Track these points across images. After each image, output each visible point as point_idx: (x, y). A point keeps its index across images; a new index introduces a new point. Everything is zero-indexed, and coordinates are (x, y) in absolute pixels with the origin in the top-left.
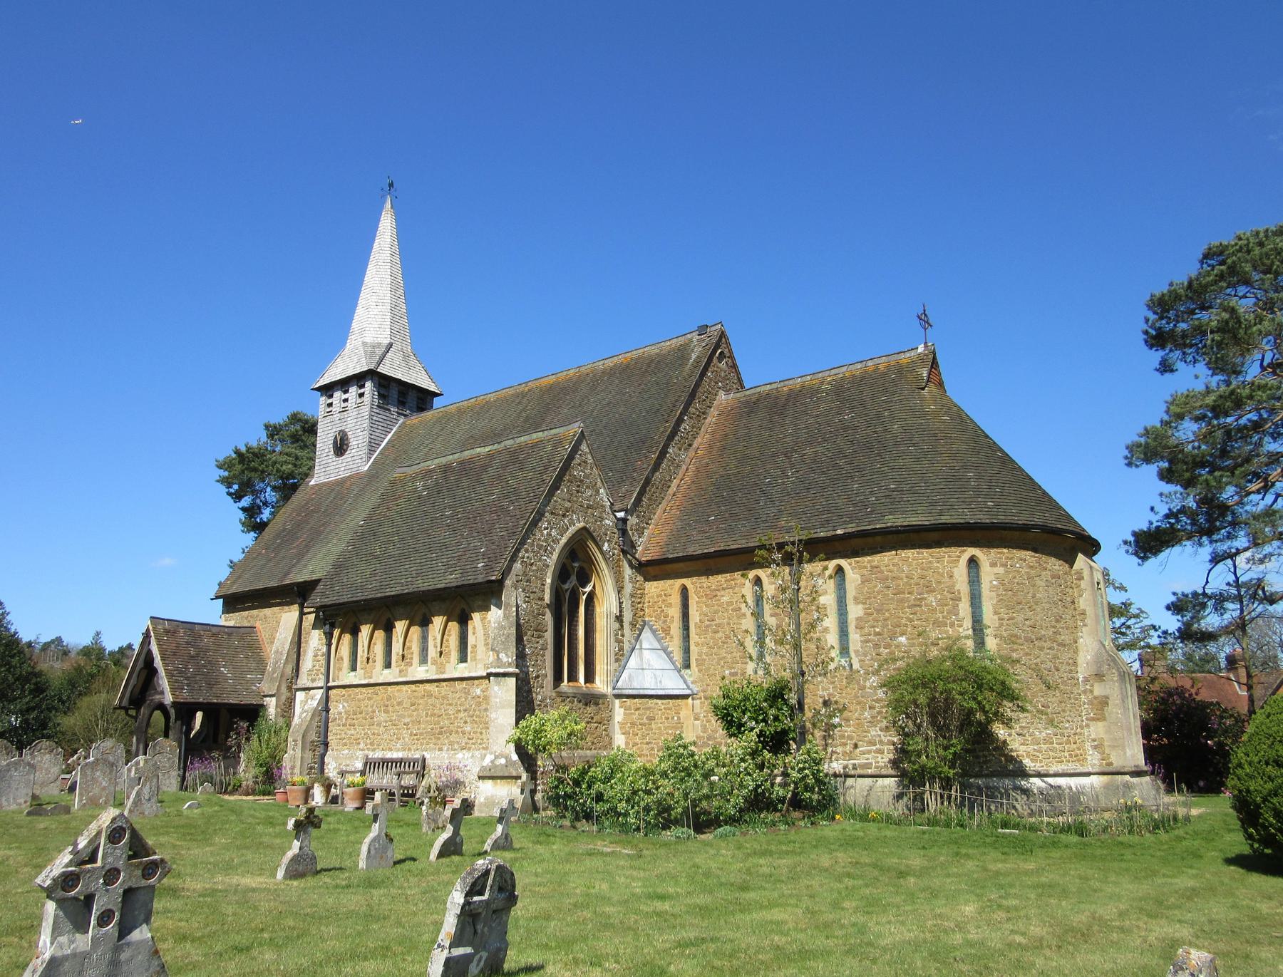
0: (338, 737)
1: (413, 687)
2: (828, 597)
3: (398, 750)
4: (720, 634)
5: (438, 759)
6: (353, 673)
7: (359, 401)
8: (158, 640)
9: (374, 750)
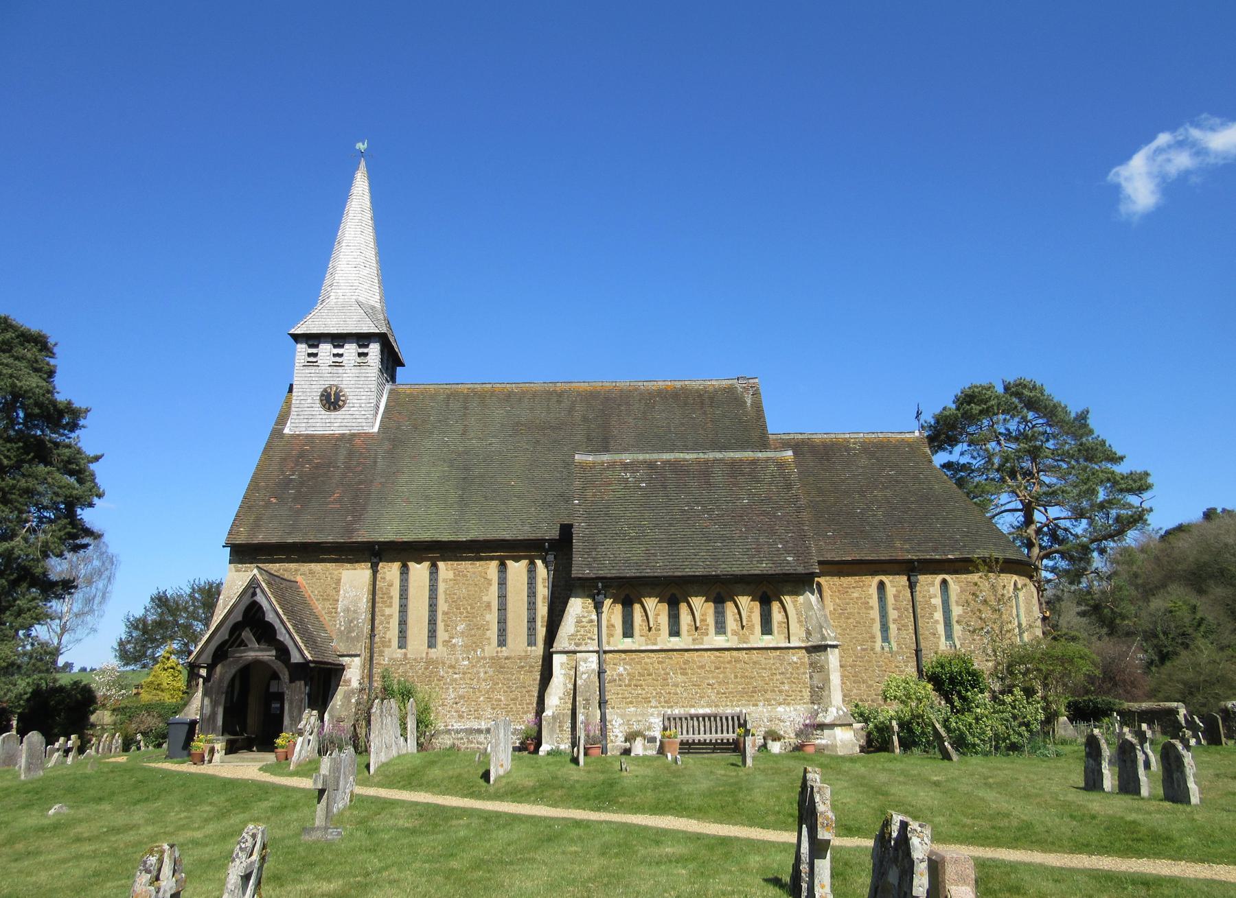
0: (620, 696)
1: (717, 653)
2: (937, 599)
3: (703, 706)
4: (851, 620)
5: (759, 715)
6: (629, 640)
7: (359, 360)
9: (672, 707)
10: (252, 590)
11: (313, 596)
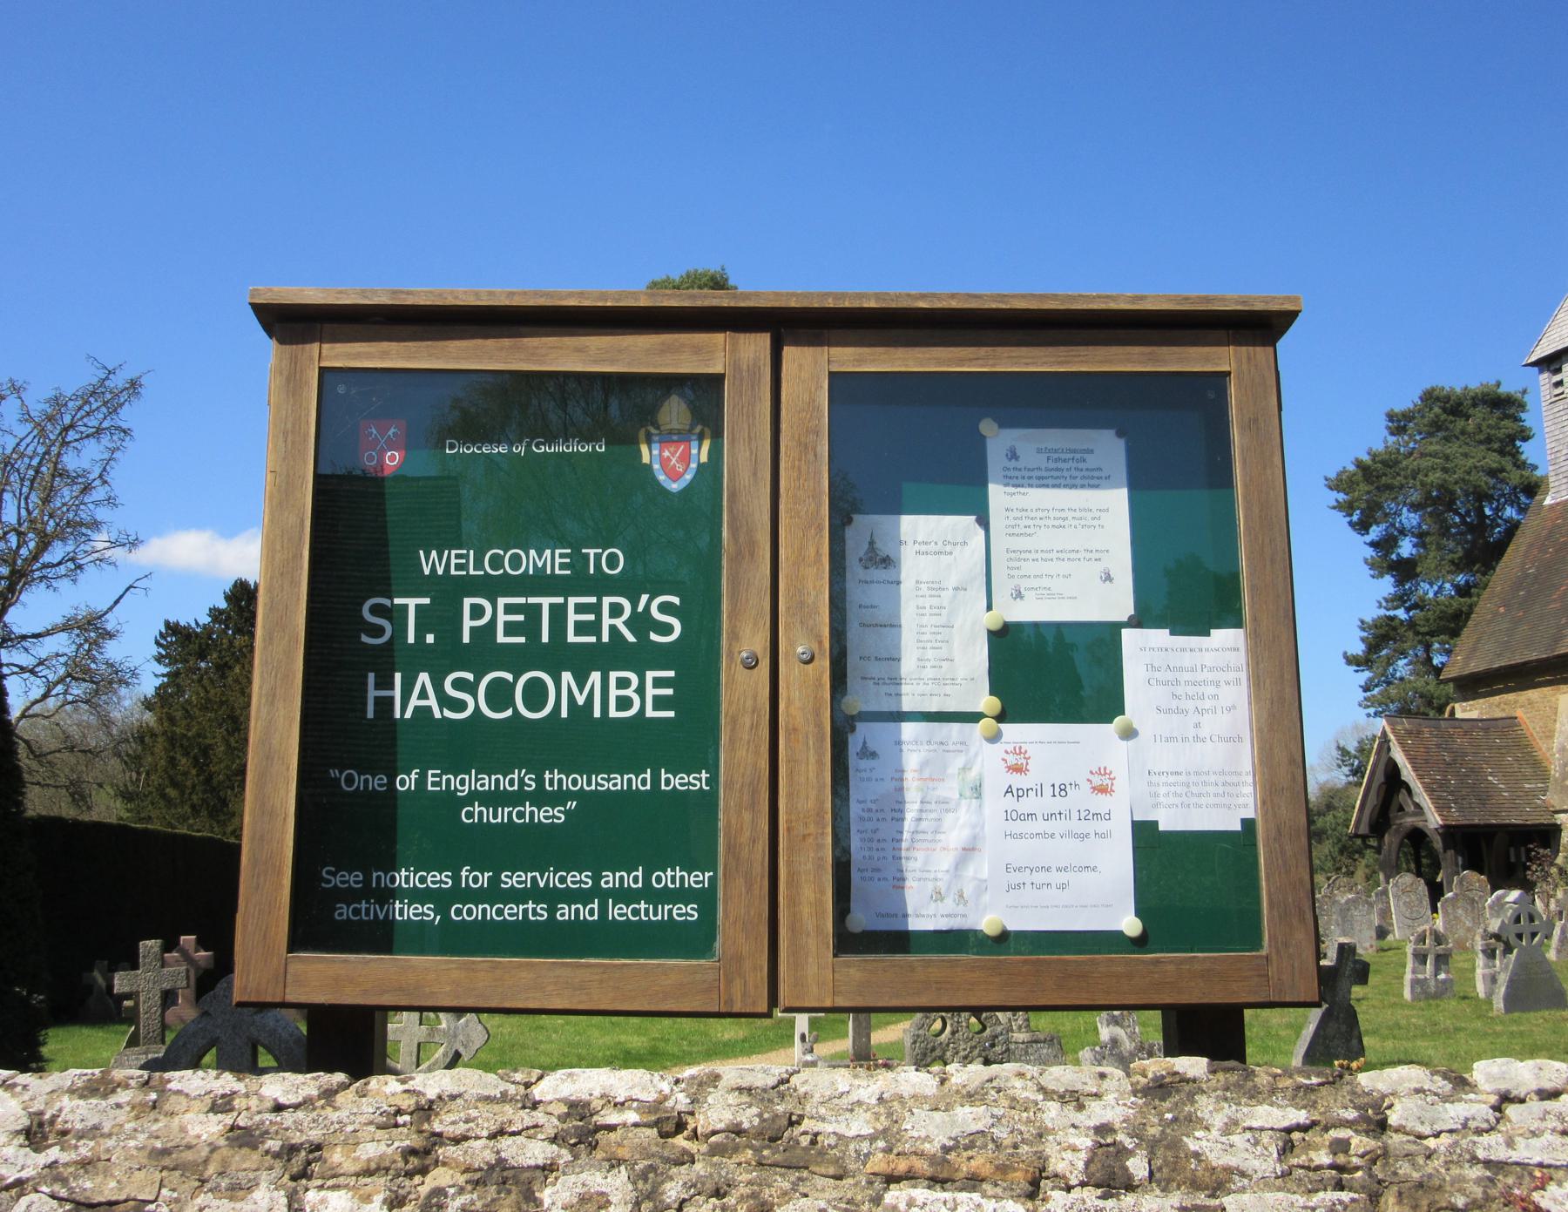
8: (1402, 745)
10: (1386, 746)
11: (1535, 734)
